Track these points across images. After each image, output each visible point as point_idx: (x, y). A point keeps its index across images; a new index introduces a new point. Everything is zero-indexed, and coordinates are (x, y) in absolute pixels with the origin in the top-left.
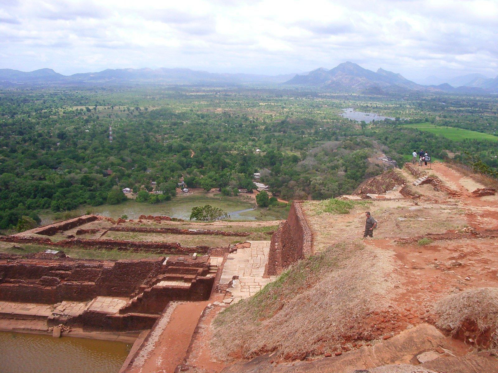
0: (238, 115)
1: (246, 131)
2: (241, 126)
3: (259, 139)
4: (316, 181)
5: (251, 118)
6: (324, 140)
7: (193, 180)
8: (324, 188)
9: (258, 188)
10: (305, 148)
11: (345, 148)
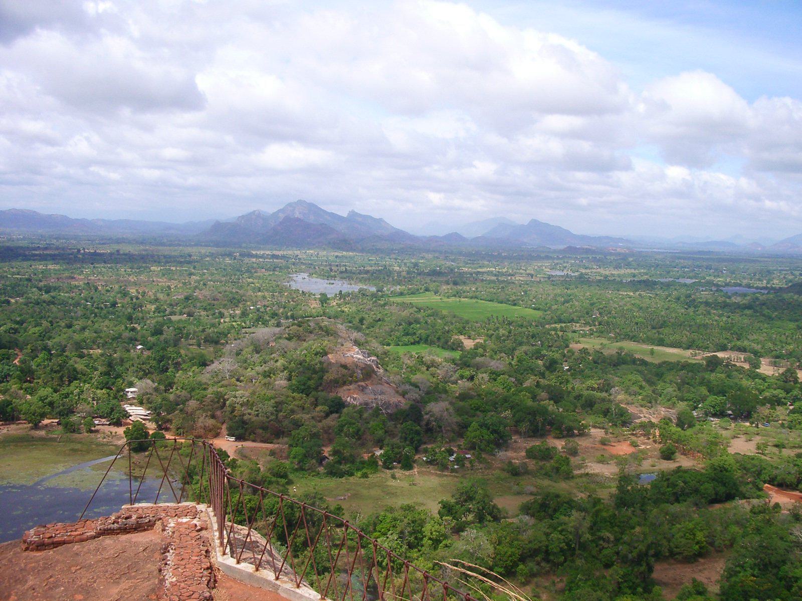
0: (112, 288)
2: (114, 305)
4: (235, 399)
7: (7, 406)
8: (249, 411)
9: (131, 416)
11: (289, 339)
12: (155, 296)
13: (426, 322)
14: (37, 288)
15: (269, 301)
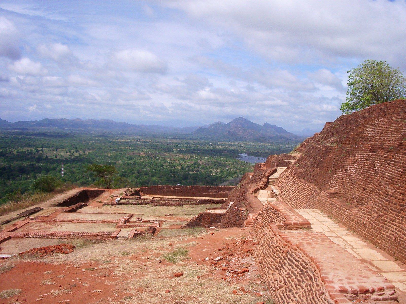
1: (167, 170)
2: (162, 166)
3: (178, 176)
5: (168, 161)
10: (214, 183)
12: (179, 163)
14: (126, 157)
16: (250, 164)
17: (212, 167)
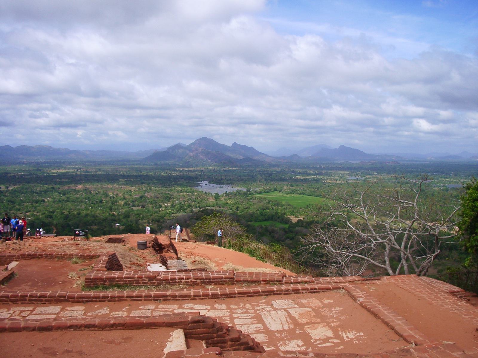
0: (99, 192)
2: (101, 201)
5: (111, 194)
6: (180, 212)
10: (161, 221)
12: (123, 196)
13: (273, 209)
14: (58, 192)
15: (186, 198)
16: (209, 195)
17: (162, 201)
